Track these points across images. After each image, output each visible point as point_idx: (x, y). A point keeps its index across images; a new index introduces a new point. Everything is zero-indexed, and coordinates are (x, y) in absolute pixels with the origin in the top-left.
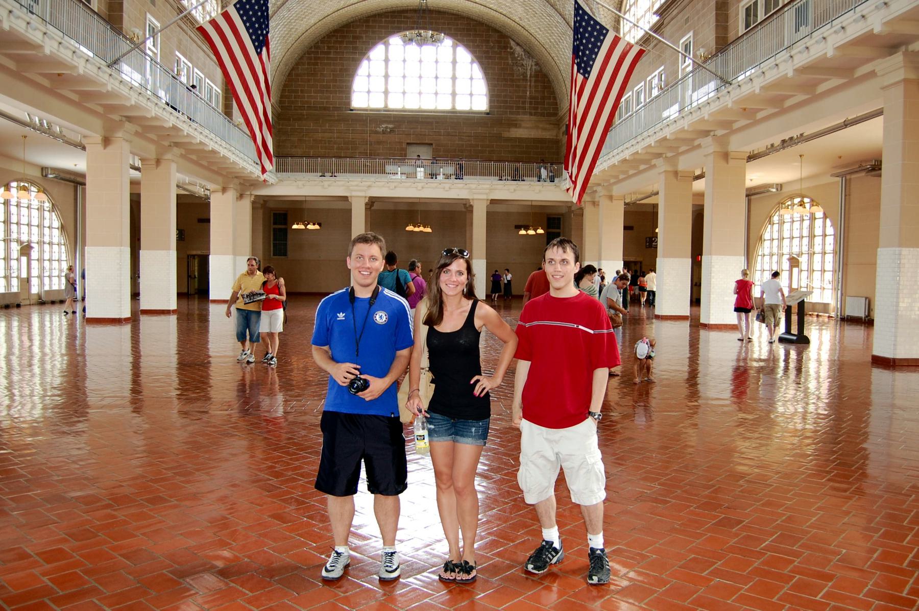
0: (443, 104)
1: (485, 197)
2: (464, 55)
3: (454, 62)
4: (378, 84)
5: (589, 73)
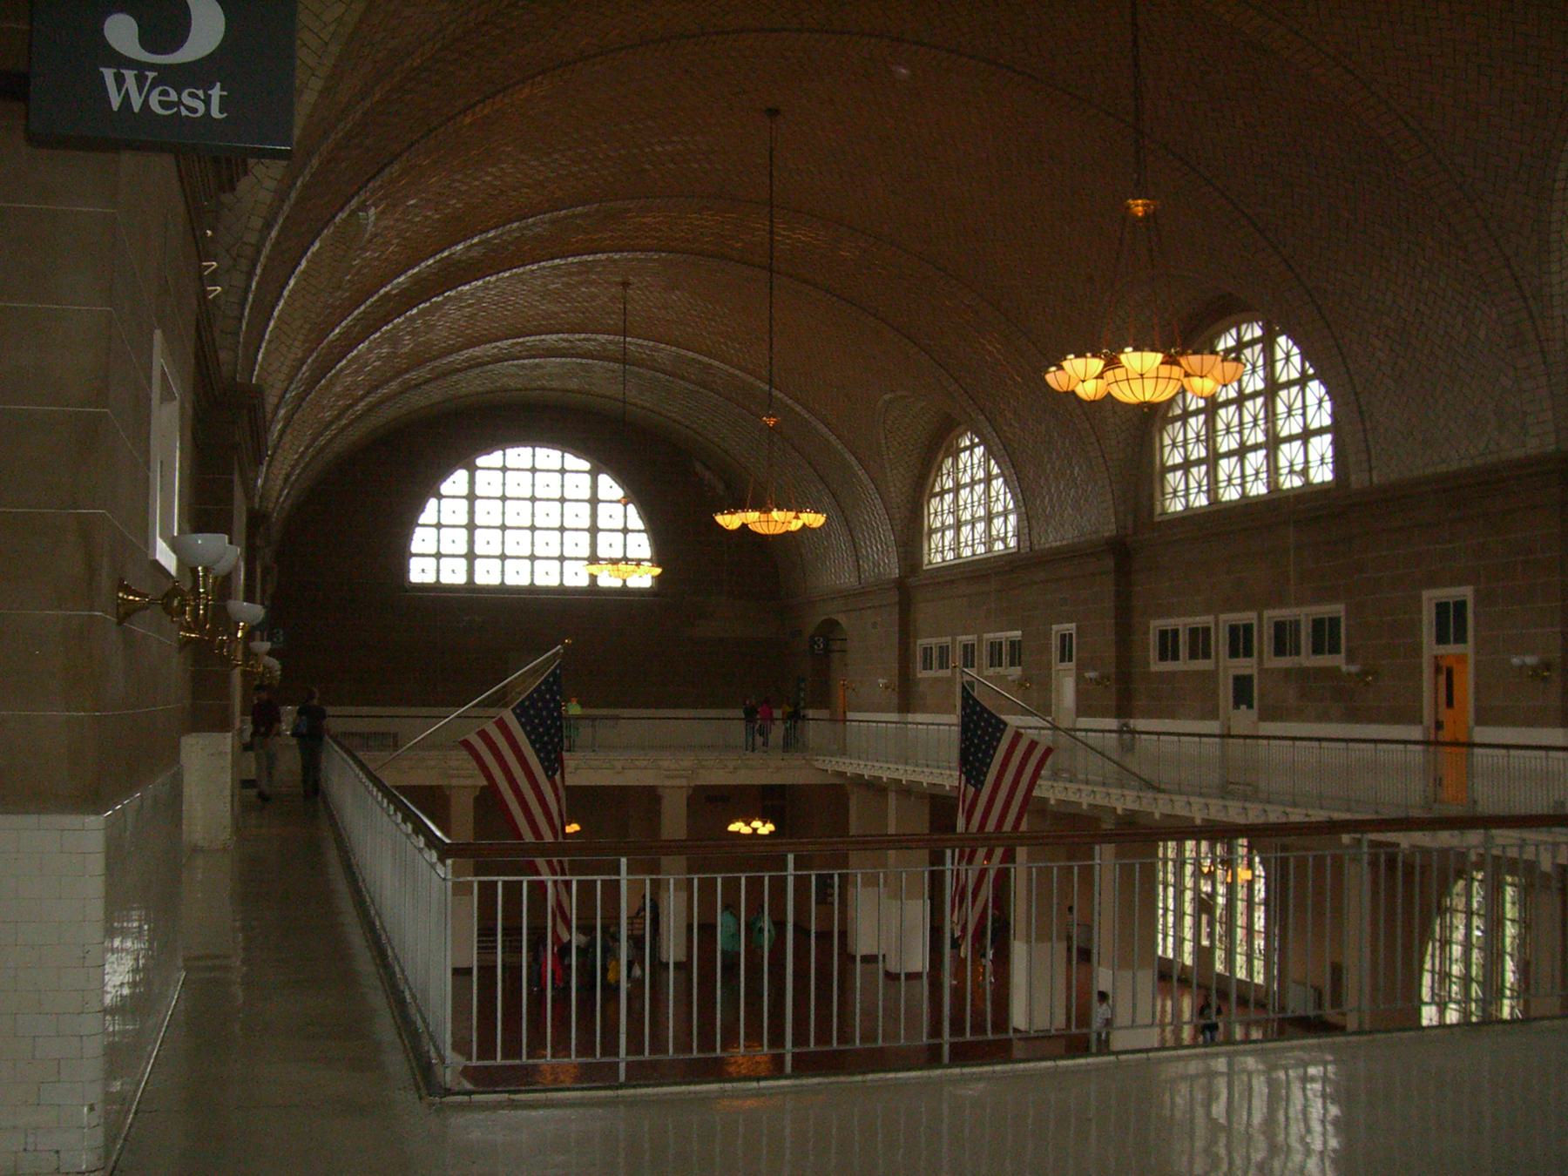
0: (577, 577)
1: (684, 782)
2: (609, 487)
3: (594, 501)
4: (455, 541)
5: (982, 783)
